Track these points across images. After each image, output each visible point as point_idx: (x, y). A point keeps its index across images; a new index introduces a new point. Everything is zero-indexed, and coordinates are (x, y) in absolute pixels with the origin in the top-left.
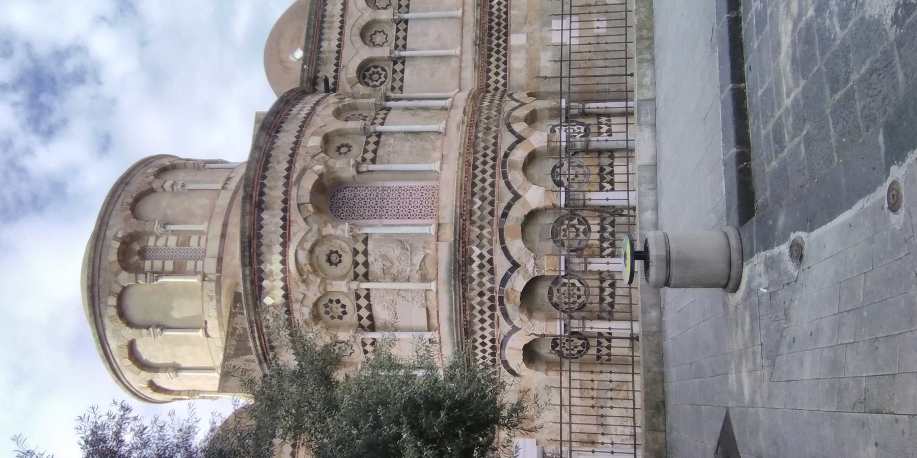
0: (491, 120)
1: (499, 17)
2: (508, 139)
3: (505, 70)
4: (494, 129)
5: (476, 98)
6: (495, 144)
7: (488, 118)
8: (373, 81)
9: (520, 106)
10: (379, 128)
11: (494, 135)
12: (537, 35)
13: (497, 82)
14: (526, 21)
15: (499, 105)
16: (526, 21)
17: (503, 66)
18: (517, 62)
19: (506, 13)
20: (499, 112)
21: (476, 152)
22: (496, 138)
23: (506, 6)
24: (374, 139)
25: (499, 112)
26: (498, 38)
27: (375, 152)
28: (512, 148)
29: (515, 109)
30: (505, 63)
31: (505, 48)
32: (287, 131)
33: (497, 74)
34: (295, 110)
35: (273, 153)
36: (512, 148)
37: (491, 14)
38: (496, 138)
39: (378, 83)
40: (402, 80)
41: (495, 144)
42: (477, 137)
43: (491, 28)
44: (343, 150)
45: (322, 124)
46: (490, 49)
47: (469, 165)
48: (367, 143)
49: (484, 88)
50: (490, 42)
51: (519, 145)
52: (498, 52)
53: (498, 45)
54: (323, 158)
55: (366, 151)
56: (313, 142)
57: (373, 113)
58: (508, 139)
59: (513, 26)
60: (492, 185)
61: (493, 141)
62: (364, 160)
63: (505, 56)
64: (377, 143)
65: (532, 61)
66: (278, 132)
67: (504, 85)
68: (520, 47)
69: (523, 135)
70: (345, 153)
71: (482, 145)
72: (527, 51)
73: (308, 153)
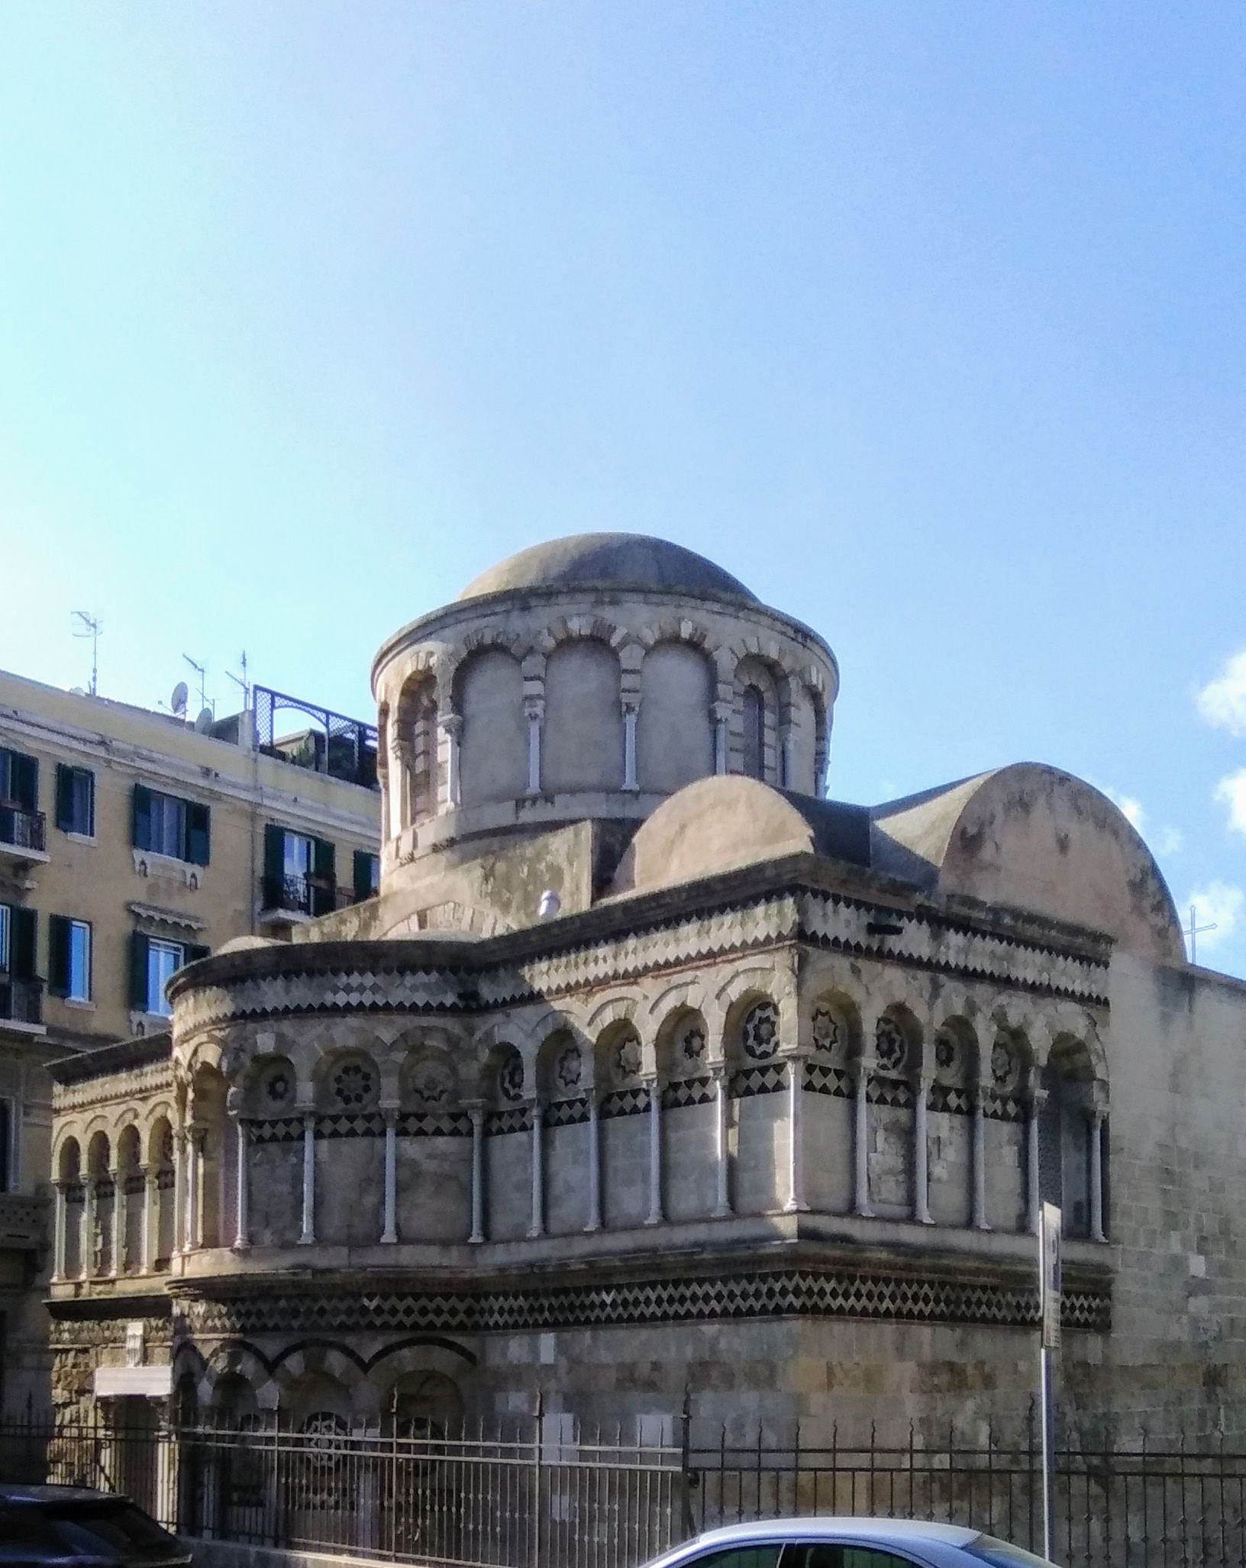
0: (315, 1317)
1: (583, 1307)
2: (271, 1347)
3: (506, 1326)
4: (295, 1323)
5: (397, 1284)
6: (265, 1328)
7: (322, 1312)
8: (512, 1075)
9: (359, 1362)
10: (309, 1136)
11: (282, 1324)
12: (552, 1385)
13: (491, 1312)
14: (575, 1362)
15: (371, 1326)
16: (575, 1362)
17: (511, 1321)
18: (516, 1349)
19: (587, 1321)
20: (343, 1328)
21: (254, 1300)
22: (276, 1328)
23: (598, 1320)
24: (294, 1129)
25: (343, 1328)
26: (551, 1308)
27: (274, 1138)
28: (260, 1356)
29: (349, 1353)
30: (516, 1326)
31: (536, 1325)
32: (287, 991)
33: (501, 1311)
34: (355, 979)
35: (249, 984)
36: (260, 1356)
37: (588, 1290)
38: (276, 1328)
39: (507, 1085)
40: (512, 1130)
41: (265, 1328)
42: (278, 1298)
43: (565, 1291)
44: (280, 1087)
45: (302, 1041)
46: (536, 1294)
47: (237, 1292)
48: (288, 1122)
49: (475, 1290)
50: (547, 1294)
51: (261, 1366)
52: (532, 1310)
53: (541, 1310)
54: (242, 1065)
55: (273, 1124)
56: (265, 1042)
57: (371, 1109)
58: (271, 1347)
59: (567, 1336)
60: (214, 1329)
61: (271, 1324)
62: (260, 1124)
63: (526, 1325)
64: (288, 1137)
65: (517, 1376)
66: (287, 975)
67: (487, 1326)
68: (535, 1351)
69: (279, 1371)
70: (286, 1090)
71: (265, 1307)
72: (530, 1366)
73: (246, 1039)
